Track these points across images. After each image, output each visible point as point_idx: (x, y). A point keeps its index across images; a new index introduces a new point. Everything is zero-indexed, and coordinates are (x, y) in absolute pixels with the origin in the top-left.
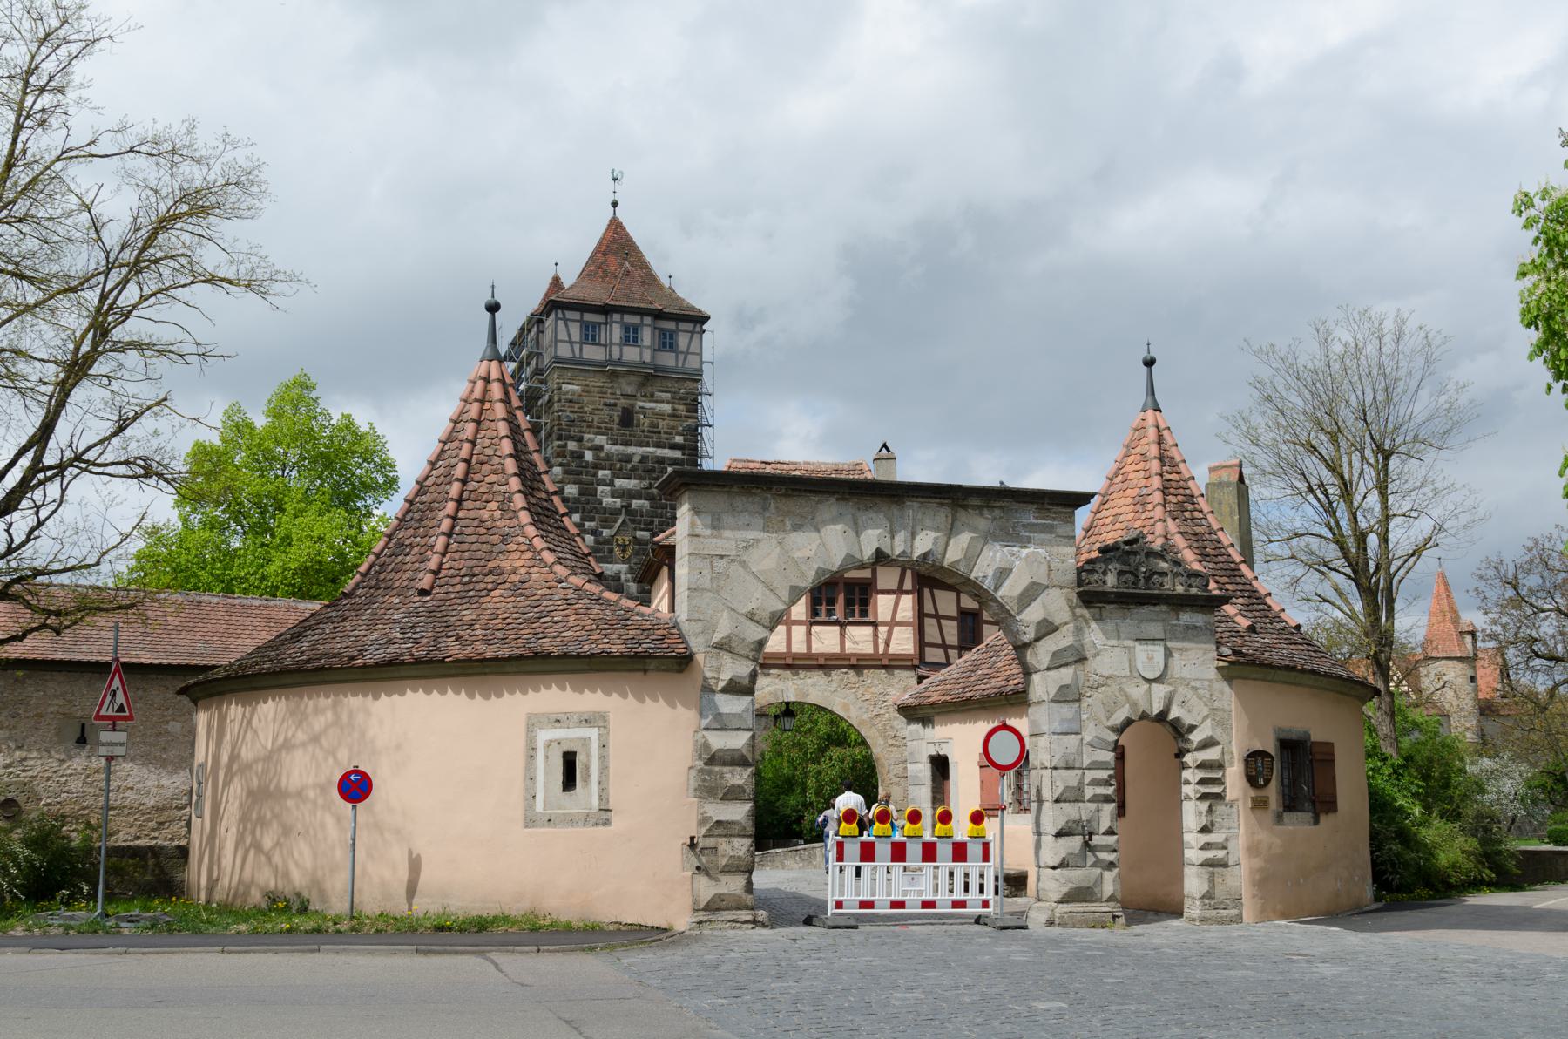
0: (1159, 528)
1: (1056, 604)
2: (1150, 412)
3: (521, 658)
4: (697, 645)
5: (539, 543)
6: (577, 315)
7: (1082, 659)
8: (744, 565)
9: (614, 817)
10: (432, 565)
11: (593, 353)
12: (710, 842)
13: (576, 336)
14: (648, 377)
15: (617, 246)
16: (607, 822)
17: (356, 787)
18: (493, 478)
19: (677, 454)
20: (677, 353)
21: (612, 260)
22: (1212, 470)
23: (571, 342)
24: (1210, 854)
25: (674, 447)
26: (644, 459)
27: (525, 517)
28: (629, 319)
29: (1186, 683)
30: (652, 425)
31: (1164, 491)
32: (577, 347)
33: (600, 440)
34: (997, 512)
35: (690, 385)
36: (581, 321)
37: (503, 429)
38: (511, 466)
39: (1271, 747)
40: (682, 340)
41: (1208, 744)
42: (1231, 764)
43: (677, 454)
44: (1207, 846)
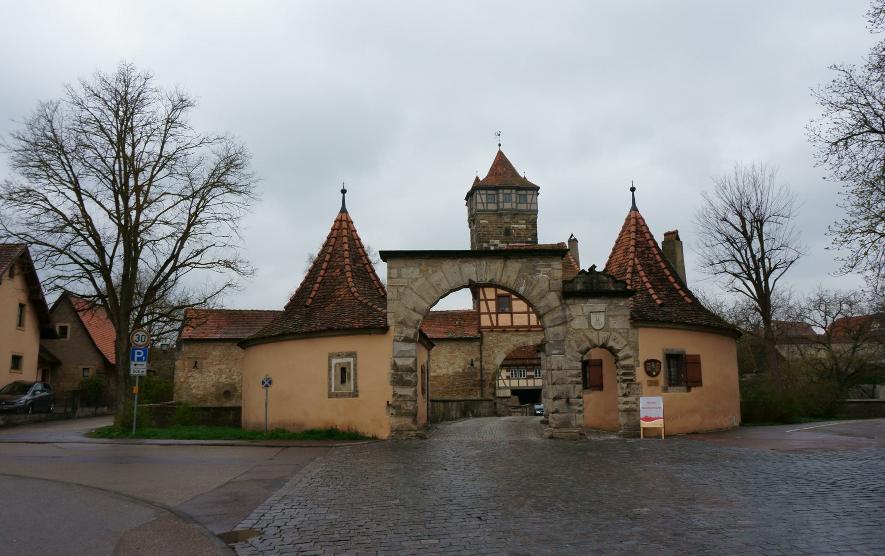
0: (631, 263)
1: (553, 299)
2: (633, 212)
3: (324, 331)
4: (390, 322)
5: (351, 284)
6: (484, 192)
7: (565, 322)
8: (412, 289)
9: (360, 395)
10: (312, 296)
11: (492, 207)
12: (398, 403)
13: (485, 201)
14: (515, 214)
15: (501, 163)
16: (357, 396)
17: (267, 383)
18: (339, 260)
20: (527, 203)
21: (499, 168)
22: (665, 235)
23: (483, 203)
24: (627, 406)
25: (527, 242)
27: (349, 274)
28: (506, 191)
29: (615, 330)
30: (518, 234)
31: (636, 246)
33: (497, 242)
34: (524, 260)
35: (533, 216)
36: (487, 194)
37: (345, 239)
38: (346, 254)
39: (660, 357)
40: (529, 198)
41: (627, 357)
42: (638, 366)
44: (626, 403)
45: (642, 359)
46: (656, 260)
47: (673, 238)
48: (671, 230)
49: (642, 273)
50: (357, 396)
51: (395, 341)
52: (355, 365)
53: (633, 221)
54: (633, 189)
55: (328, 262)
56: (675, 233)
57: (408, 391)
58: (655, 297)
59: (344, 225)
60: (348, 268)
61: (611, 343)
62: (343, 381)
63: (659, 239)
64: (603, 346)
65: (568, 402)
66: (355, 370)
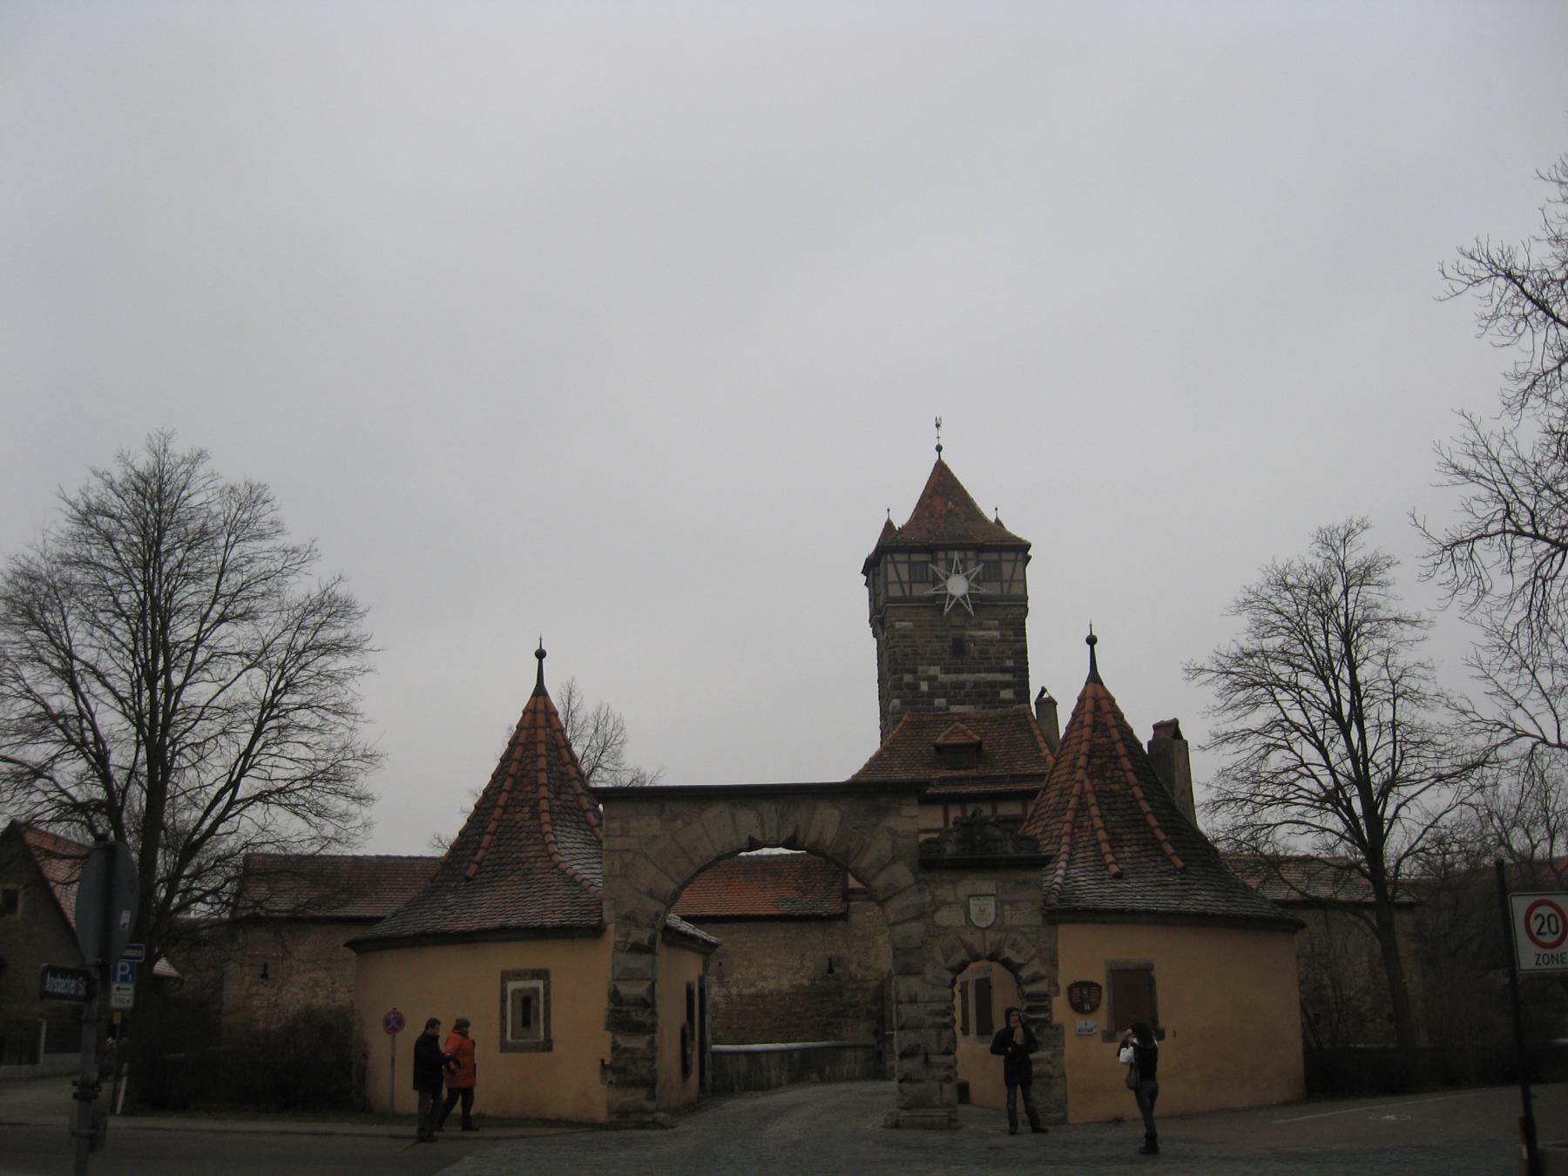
0: (1076, 790)
1: (902, 873)
6: (904, 557)
8: (646, 857)
10: (478, 858)
13: (905, 578)
16: (550, 1049)
19: (1008, 677)
20: (1001, 581)
22: (1156, 727)
23: (901, 582)
25: (1004, 670)
26: (976, 684)
31: (1090, 755)
32: (906, 587)
33: (934, 670)
36: (910, 563)
37: (542, 749)
38: (543, 778)
39: (1100, 977)
40: (1007, 569)
42: (1057, 993)
43: (1008, 677)
45: (1064, 981)
46: (1127, 783)
47: (1169, 733)
48: (1166, 719)
49: (1094, 811)
50: (550, 1049)
51: (617, 948)
52: (547, 993)
53: (1089, 704)
54: (1092, 641)
55: (509, 792)
56: (1174, 724)
57: (639, 1043)
58: (1110, 858)
59: (541, 721)
60: (544, 805)
61: (1008, 953)
62: (526, 1023)
63: (1144, 735)
64: (993, 957)
65: (926, 1060)
66: (547, 1002)
